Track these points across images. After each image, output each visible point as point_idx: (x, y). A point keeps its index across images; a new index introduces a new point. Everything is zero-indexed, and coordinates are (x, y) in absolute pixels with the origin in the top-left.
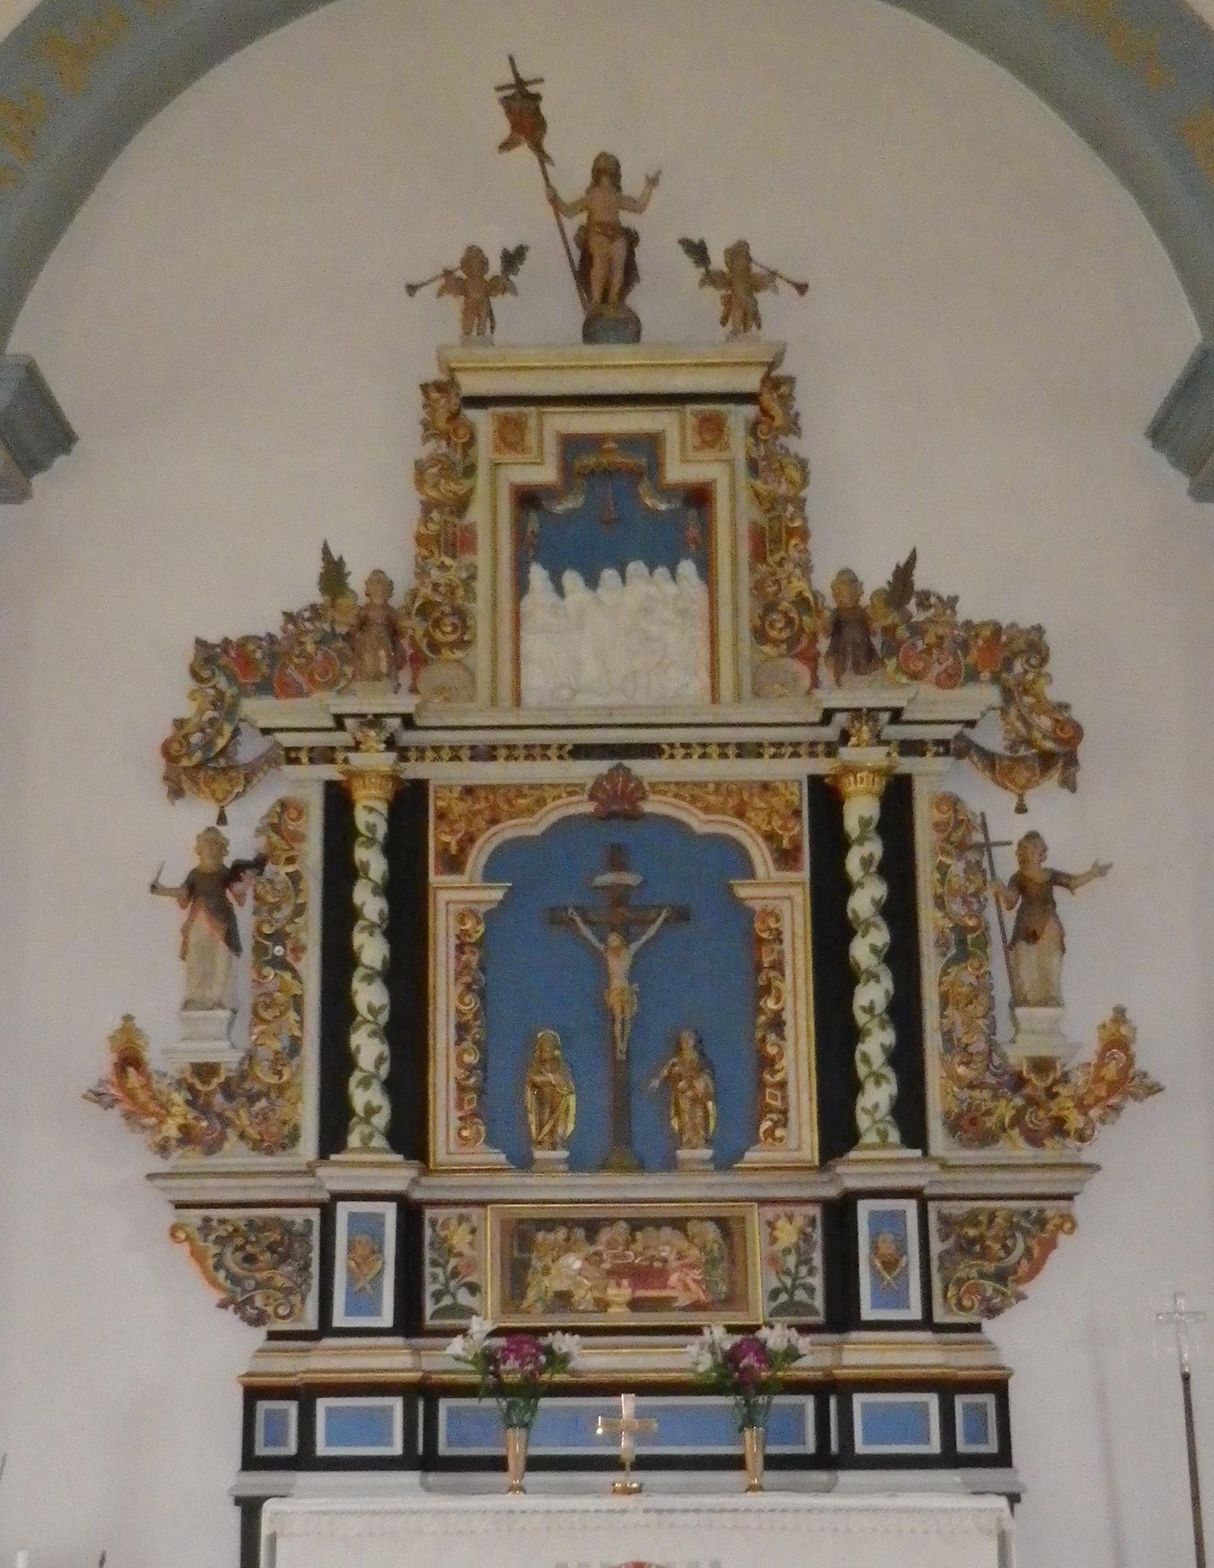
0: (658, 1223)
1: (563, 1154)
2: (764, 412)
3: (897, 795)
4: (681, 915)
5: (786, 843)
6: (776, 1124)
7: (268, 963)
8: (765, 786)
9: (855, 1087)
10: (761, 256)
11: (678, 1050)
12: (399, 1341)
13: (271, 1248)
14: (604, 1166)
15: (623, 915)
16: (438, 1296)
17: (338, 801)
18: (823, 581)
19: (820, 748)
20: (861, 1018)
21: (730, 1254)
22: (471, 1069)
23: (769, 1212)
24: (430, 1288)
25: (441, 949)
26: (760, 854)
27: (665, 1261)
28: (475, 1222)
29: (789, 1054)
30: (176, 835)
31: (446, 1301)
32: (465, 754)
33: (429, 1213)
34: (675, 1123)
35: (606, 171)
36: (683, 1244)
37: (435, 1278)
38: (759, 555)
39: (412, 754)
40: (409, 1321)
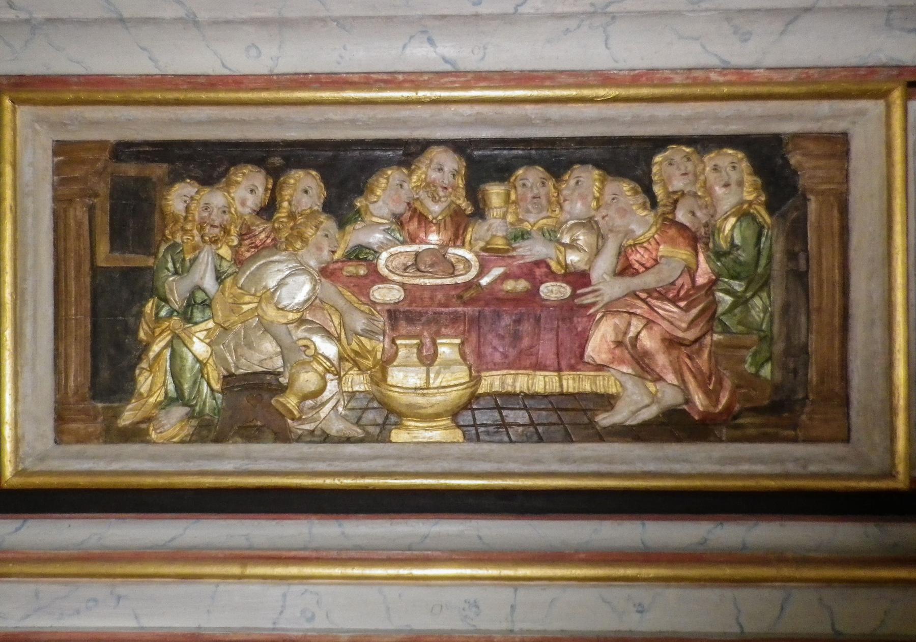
0: (557, 157)
21: (791, 256)
27: (579, 279)
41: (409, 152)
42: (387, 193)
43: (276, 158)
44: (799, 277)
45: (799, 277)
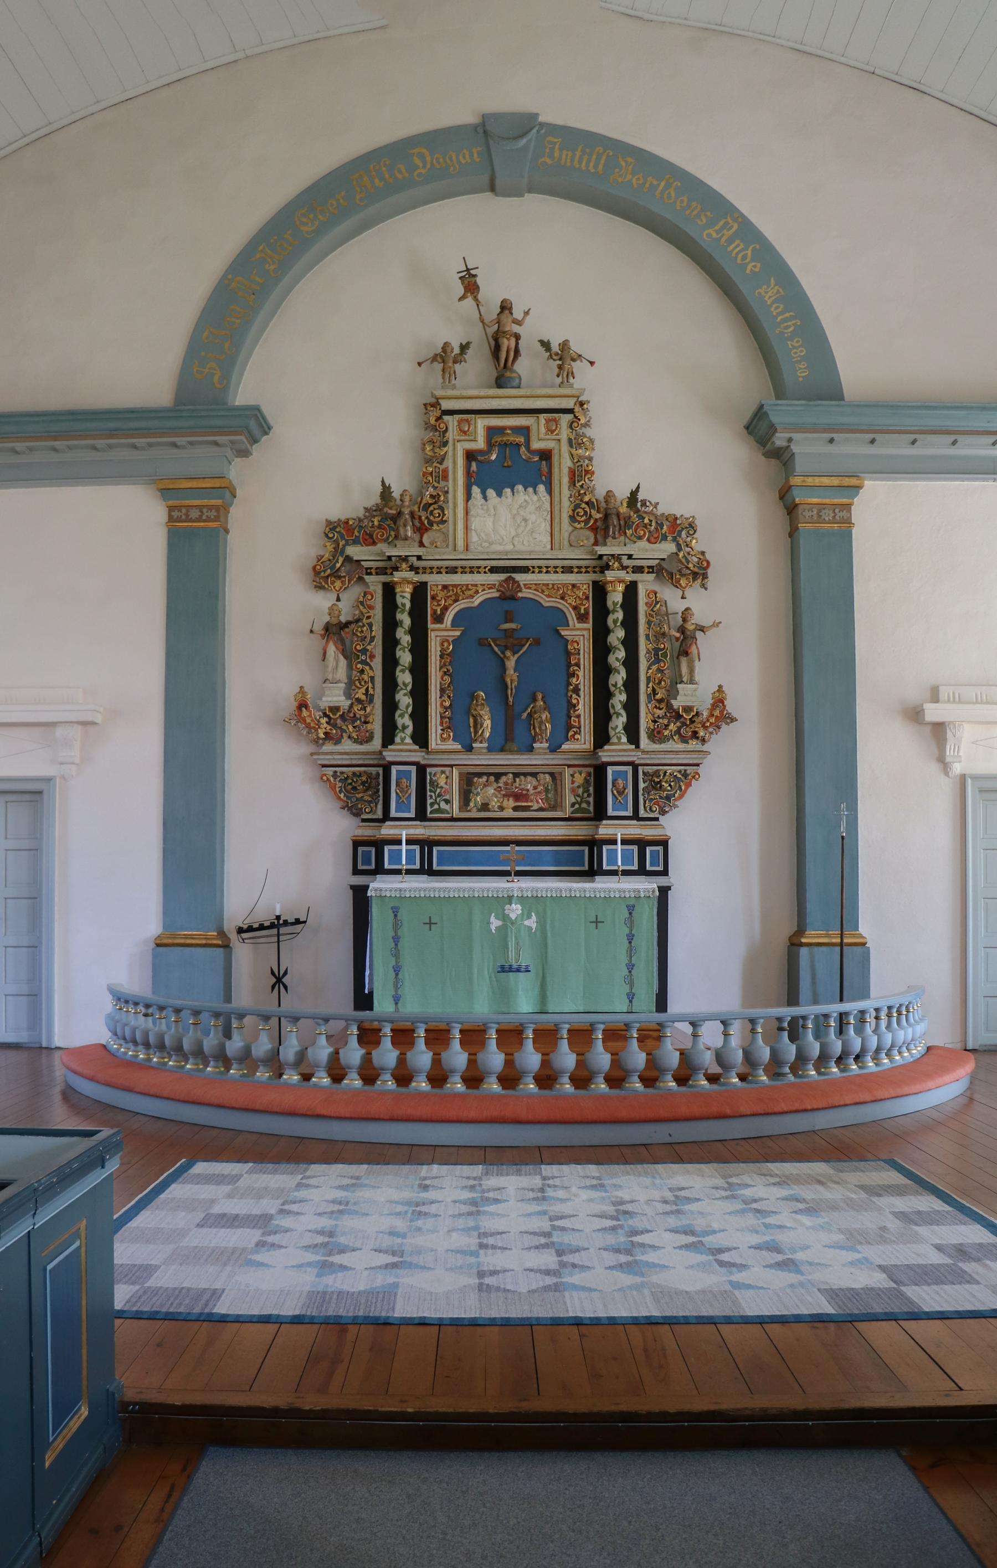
0: (525, 775)
1: (486, 745)
2: (576, 417)
3: (631, 589)
4: (537, 642)
5: (582, 611)
6: (575, 733)
7: (359, 663)
8: (574, 586)
9: (608, 717)
10: (575, 347)
11: (534, 699)
12: (418, 823)
13: (363, 783)
14: (502, 750)
15: (511, 642)
16: (432, 804)
17: (389, 591)
18: (600, 493)
19: (597, 569)
20: (612, 689)
22: (446, 708)
23: (572, 770)
24: (429, 801)
25: (433, 657)
26: (571, 616)
27: (528, 790)
28: (447, 773)
29: (581, 702)
30: (321, 604)
31: (436, 806)
32: (443, 570)
33: (428, 770)
34: (533, 732)
35: (505, 307)
36: (535, 783)
37: (431, 797)
38: (573, 482)
39: (421, 571)
40: (421, 815)
41: (505, 774)
42: (504, 779)
43: (489, 774)
44: (556, 790)
45: (556, 790)
